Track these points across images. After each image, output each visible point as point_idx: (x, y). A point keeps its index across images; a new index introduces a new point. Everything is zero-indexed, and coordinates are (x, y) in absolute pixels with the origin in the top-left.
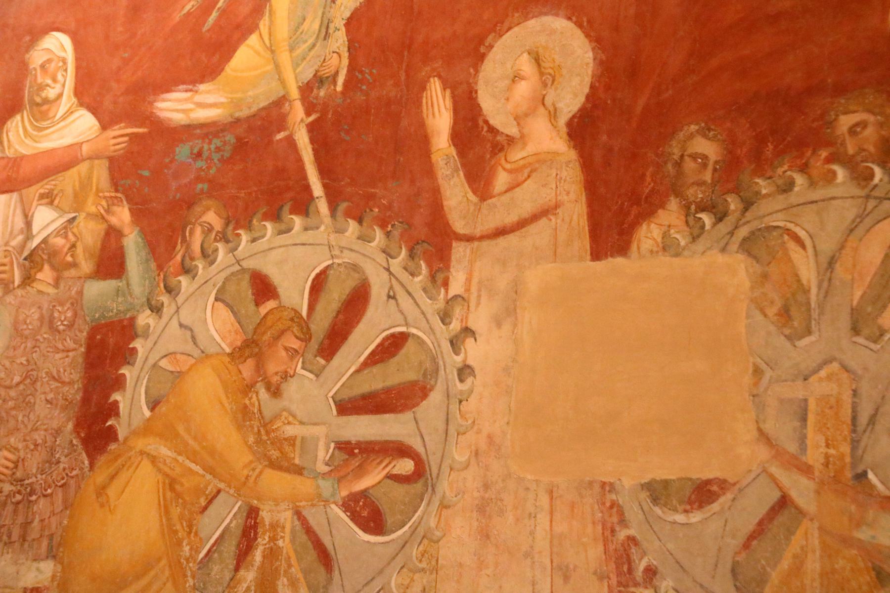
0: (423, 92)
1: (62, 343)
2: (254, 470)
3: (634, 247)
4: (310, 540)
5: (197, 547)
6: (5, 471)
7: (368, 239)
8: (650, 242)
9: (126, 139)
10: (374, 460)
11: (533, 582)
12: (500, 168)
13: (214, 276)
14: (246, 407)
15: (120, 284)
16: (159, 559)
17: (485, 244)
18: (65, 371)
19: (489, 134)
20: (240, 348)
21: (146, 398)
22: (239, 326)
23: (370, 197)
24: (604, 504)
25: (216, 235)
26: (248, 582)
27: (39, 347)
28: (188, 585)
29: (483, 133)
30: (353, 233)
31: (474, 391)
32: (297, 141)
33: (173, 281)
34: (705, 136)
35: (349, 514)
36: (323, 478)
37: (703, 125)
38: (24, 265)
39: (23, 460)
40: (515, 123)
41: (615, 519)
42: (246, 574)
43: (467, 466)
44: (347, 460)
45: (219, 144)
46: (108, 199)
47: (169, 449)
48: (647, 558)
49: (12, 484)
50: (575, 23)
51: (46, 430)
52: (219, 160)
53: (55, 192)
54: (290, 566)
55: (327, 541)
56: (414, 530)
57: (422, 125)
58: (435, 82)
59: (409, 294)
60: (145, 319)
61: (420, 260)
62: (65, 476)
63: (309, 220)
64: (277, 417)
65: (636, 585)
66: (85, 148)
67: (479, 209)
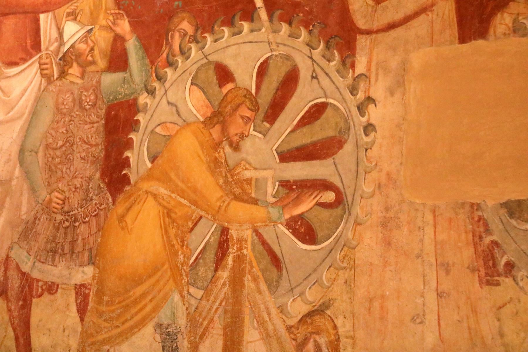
1: (89, 118)
2: (224, 202)
3: (491, 31)
4: (265, 249)
5: (188, 256)
6: (57, 206)
8: (503, 27)
11: (424, 274)
14: (216, 159)
15: (126, 75)
16: (163, 265)
17: (380, 36)
18: (92, 137)
20: (210, 118)
21: (148, 154)
22: (208, 102)
24: (473, 218)
25: (190, 38)
26: (224, 278)
28: (183, 281)
30: (285, 33)
31: (376, 142)
33: (161, 72)
35: (291, 231)
36: (272, 207)
38: (60, 64)
39: (68, 198)
41: (482, 229)
42: (223, 273)
43: (373, 195)
44: (288, 193)
46: (114, 15)
47: (166, 189)
48: (506, 256)
49: (62, 215)
51: (82, 178)
53: (77, 11)
54: (252, 267)
55: (276, 249)
56: (337, 241)
59: (327, 74)
60: (143, 99)
61: (334, 49)
63: (254, 24)
64: (238, 165)
65: (499, 275)
67: (376, 11)
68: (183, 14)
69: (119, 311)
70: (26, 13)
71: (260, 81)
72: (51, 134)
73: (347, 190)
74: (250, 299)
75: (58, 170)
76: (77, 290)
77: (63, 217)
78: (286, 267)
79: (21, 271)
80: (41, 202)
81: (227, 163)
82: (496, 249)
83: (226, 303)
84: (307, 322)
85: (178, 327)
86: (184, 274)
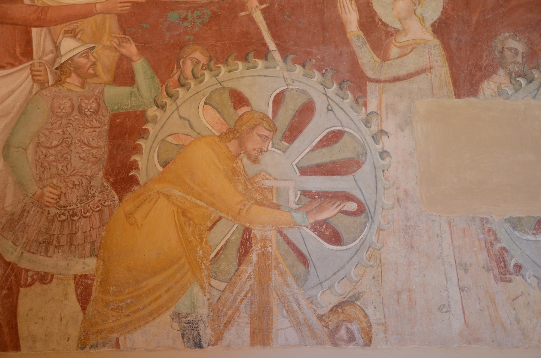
2: (245, 205)
3: (481, 93)
6: (51, 200)
7: (311, 77)
9: (130, 4)
10: (329, 202)
12: (392, 45)
13: (203, 90)
14: (234, 168)
15: (133, 90)
16: (180, 259)
17: (388, 85)
18: (93, 140)
19: (383, 26)
23: (309, 53)
25: (202, 66)
26: (249, 272)
27: (72, 124)
28: (203, 274)
29: (379, 25)
31: (391, 165)
32: (255, 18)
33: (172, 91)
34: (514, 39)
35: (316, 233)
36: (296, 212)
37: (512, 33)
38: (56, 74)
39: (65, 194)
40: (399, 22)
41: (492, 238)
43: (393, 207)
45: (199, 14)
46: (119, 38)
48: (514, 259)
51: (81, 176)
52: (200, 23)
53: (77, 30)
54: (278, 263)
57: (339, 17)
60: (153, 111)
61: (346, 91)
62: (100, 205)
64: (258, 174)
66: (98, 7)
67: (382, 66)
68: (195, 46)
69: (129, 301)
70: (14, 24)
71: (276, 108)
72: (44, 134)
73: (368, 202)
74: (278, 291)
75: (52, 167)
76: (77, 280)
77: (57, 211)
78: (313, 264)
79: (5, 260)
80: (31, 195)
81: (245, 172)
82: (505, 253)
83: (252, 295)
84: (338, 311)
85: (200, 316)
86: (204, 268)
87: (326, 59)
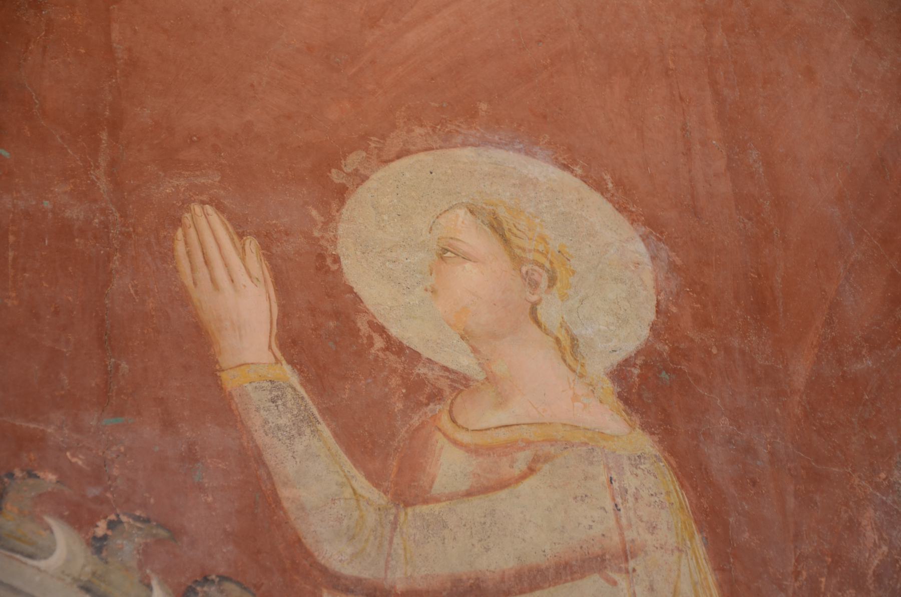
0: (175, 228)
7: (30, 549)
19: (392, 357)
29: (373, 351)
40: (464, 344)
50: (584, 179)
57: (183, 298)
58: (206, 215)
67: (395, 524)
87: (115, 472)
